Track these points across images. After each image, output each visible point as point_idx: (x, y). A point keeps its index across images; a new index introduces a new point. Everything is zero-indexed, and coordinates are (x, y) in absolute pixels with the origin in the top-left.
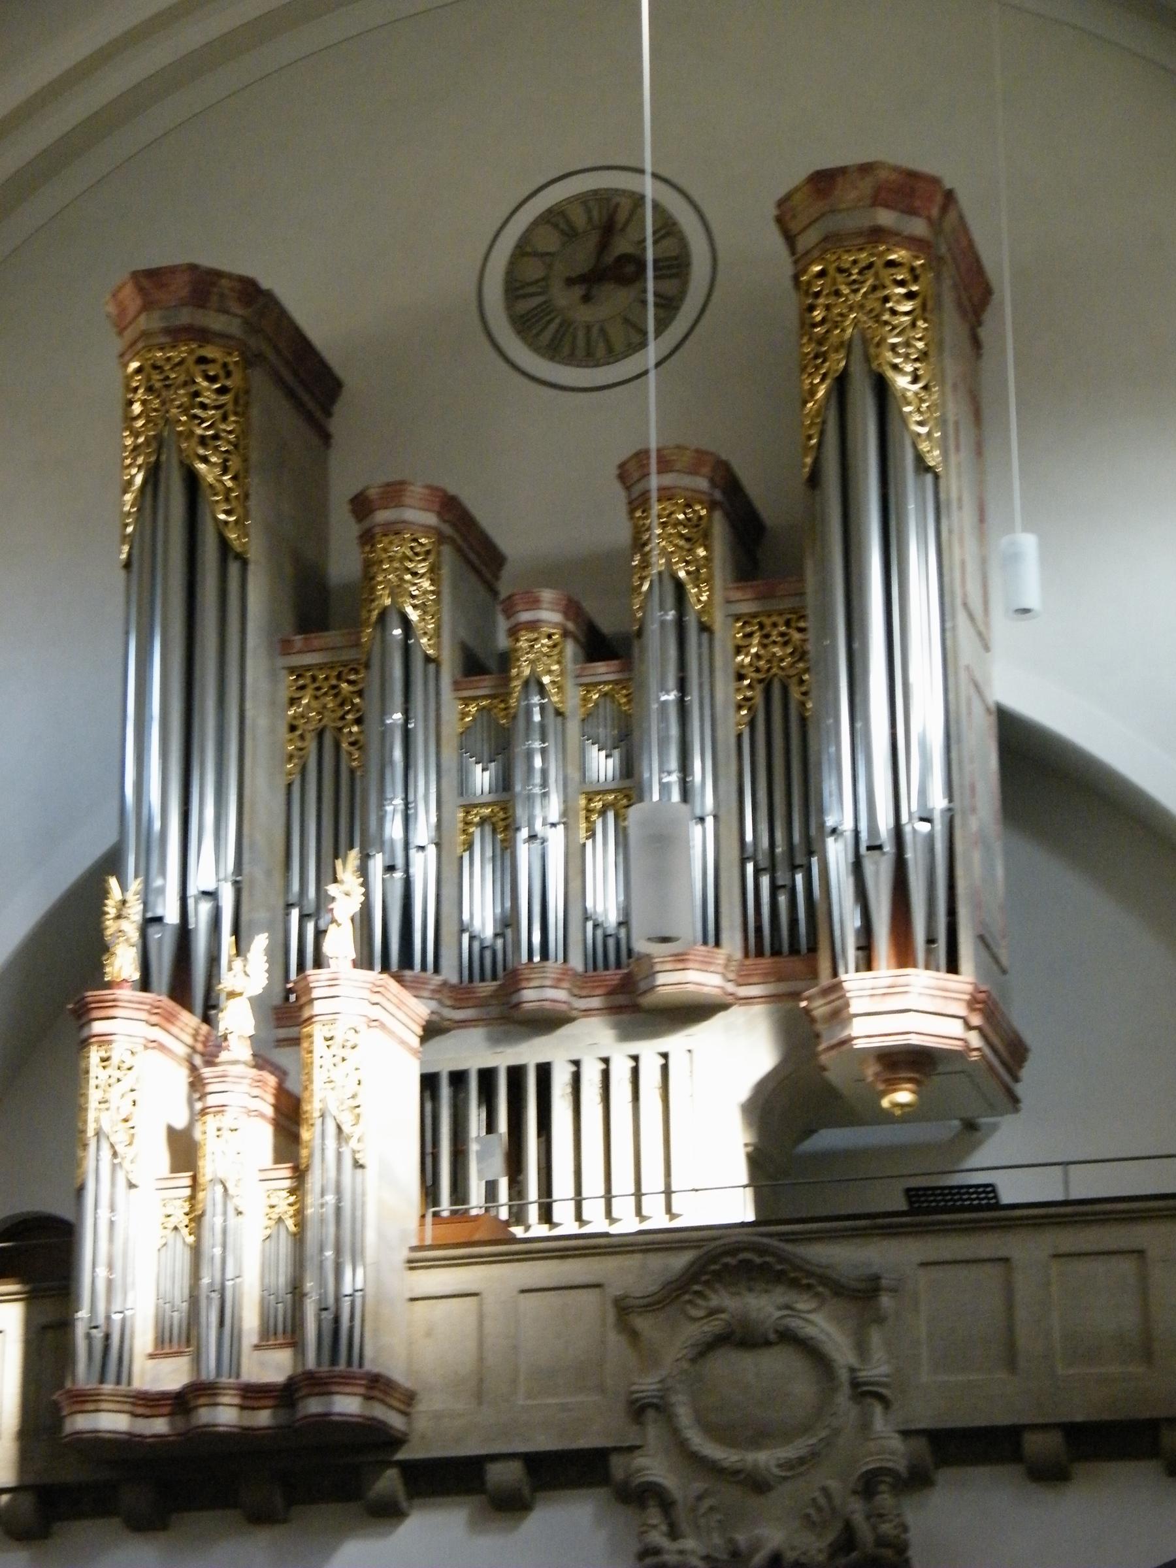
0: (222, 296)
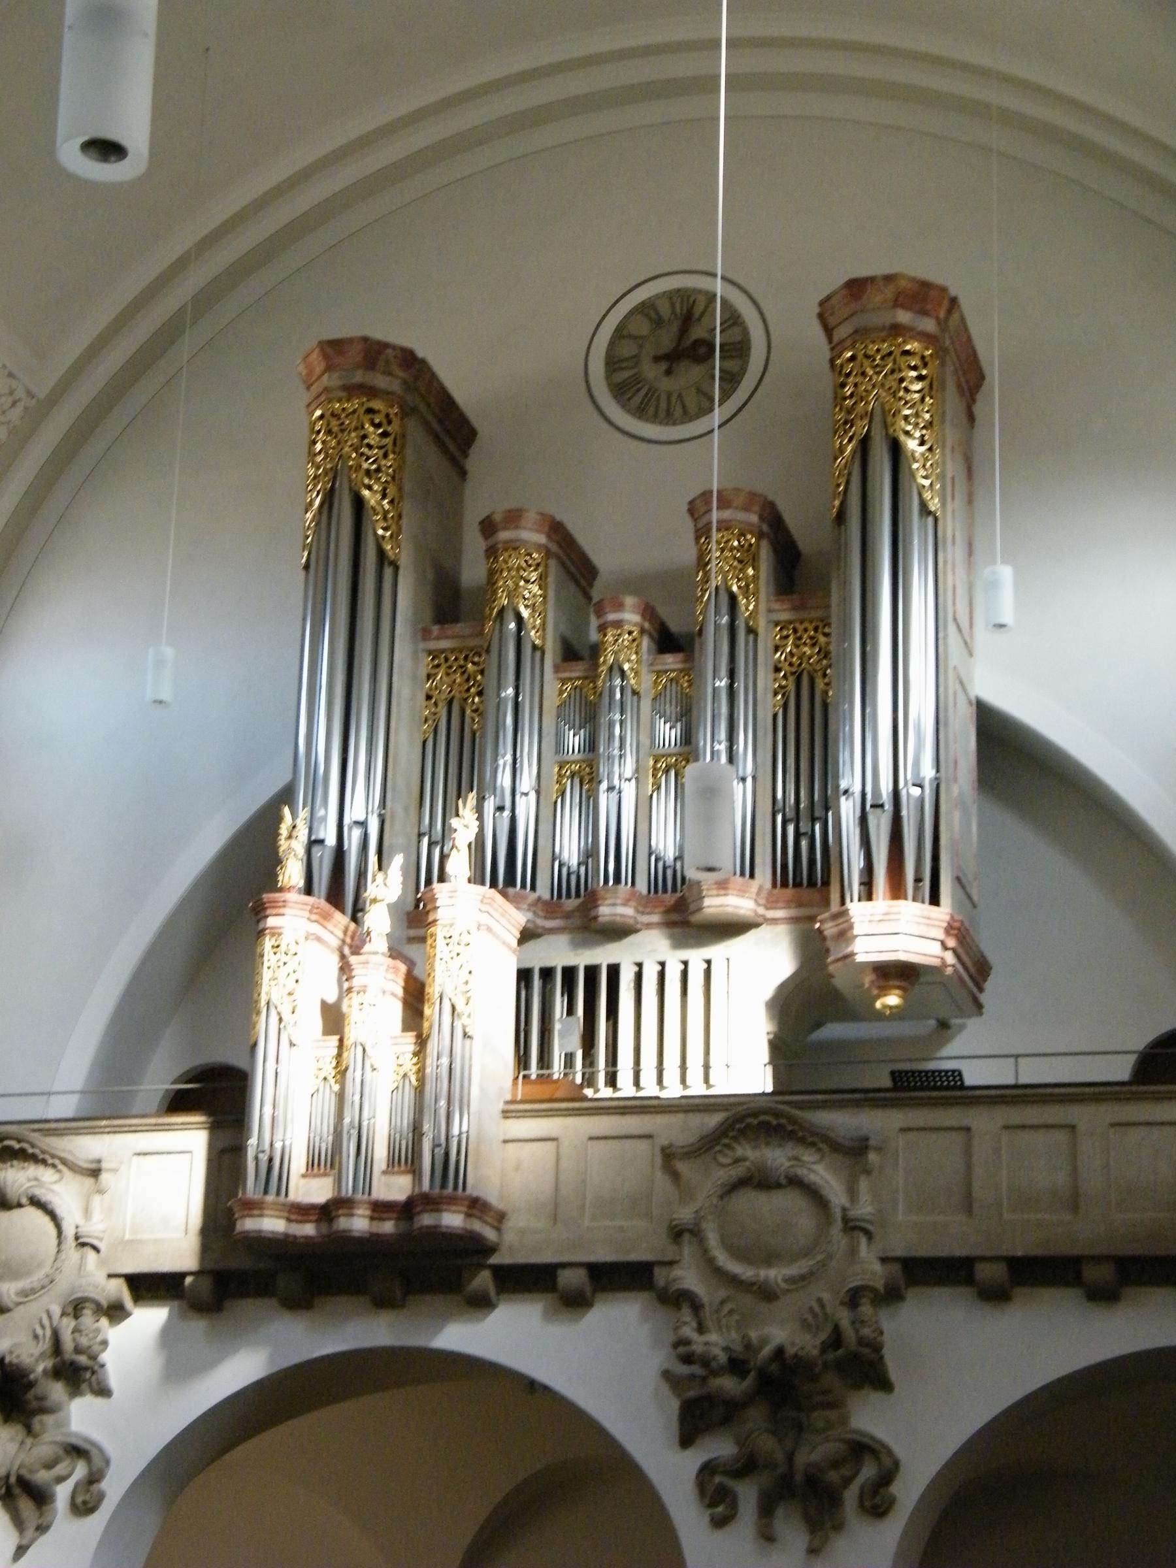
0: (387, 362)
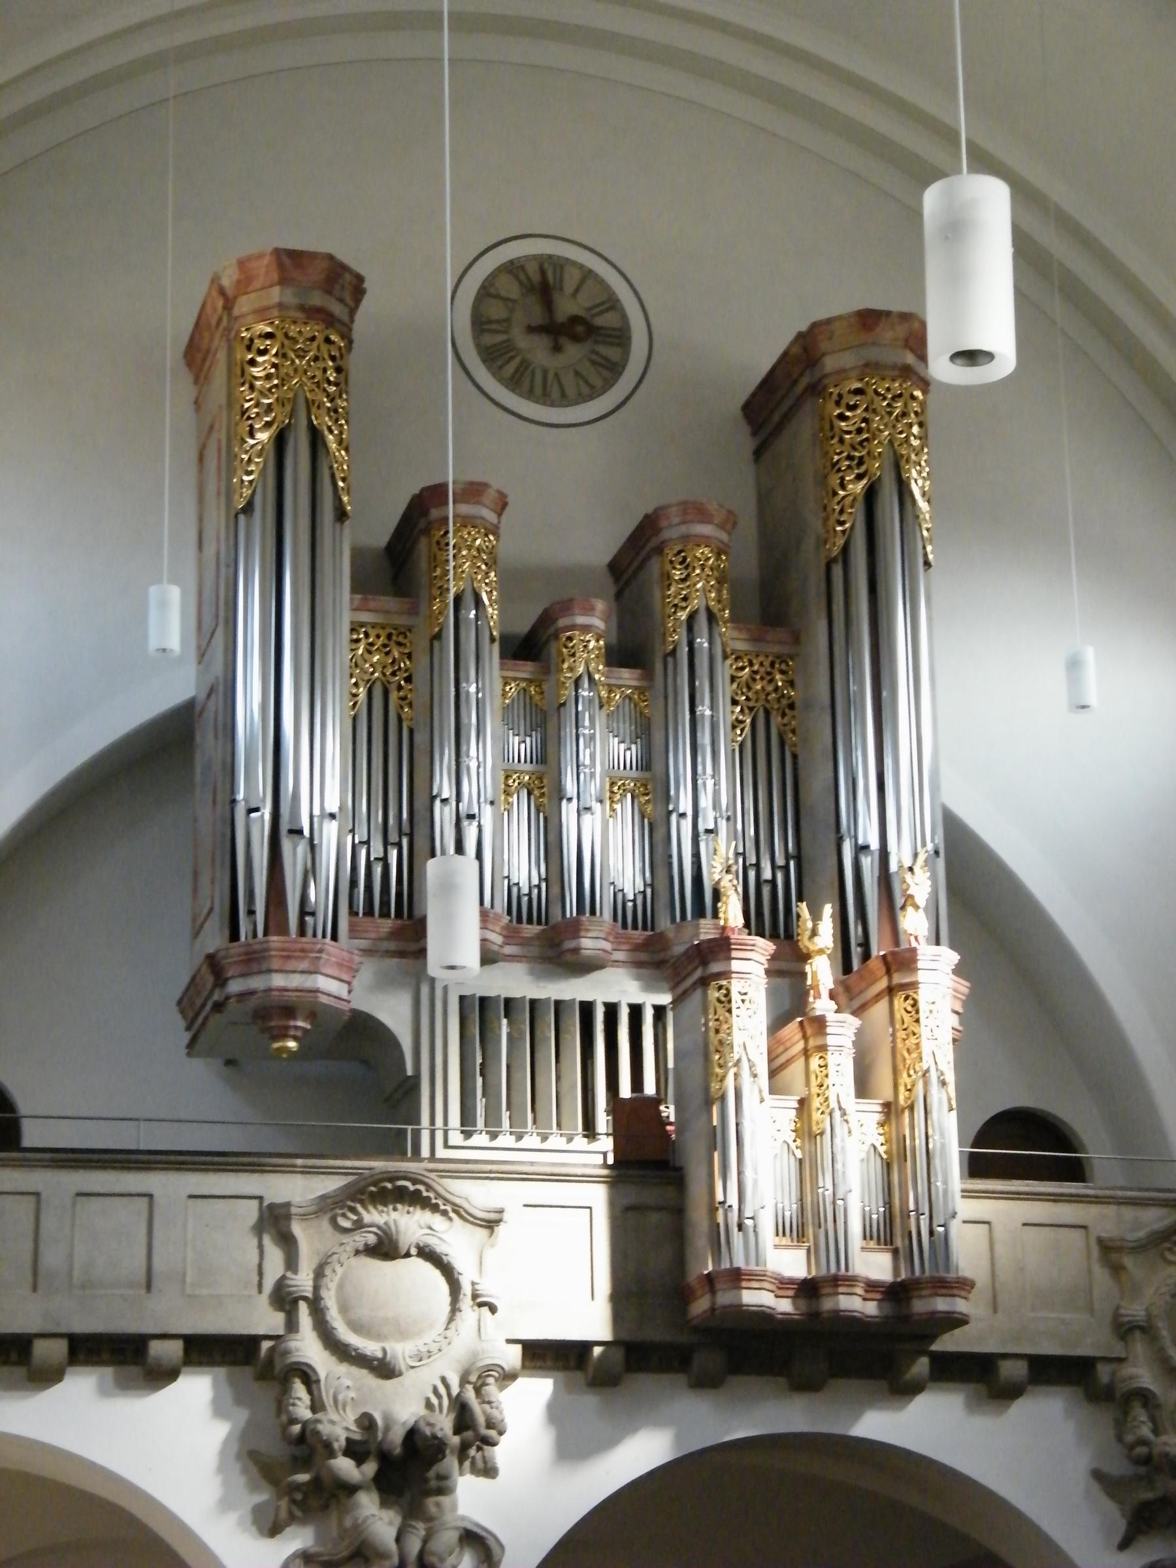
0: (343, 287)
